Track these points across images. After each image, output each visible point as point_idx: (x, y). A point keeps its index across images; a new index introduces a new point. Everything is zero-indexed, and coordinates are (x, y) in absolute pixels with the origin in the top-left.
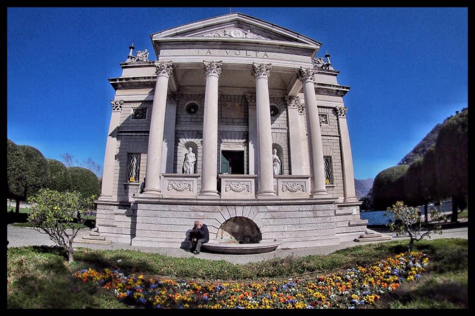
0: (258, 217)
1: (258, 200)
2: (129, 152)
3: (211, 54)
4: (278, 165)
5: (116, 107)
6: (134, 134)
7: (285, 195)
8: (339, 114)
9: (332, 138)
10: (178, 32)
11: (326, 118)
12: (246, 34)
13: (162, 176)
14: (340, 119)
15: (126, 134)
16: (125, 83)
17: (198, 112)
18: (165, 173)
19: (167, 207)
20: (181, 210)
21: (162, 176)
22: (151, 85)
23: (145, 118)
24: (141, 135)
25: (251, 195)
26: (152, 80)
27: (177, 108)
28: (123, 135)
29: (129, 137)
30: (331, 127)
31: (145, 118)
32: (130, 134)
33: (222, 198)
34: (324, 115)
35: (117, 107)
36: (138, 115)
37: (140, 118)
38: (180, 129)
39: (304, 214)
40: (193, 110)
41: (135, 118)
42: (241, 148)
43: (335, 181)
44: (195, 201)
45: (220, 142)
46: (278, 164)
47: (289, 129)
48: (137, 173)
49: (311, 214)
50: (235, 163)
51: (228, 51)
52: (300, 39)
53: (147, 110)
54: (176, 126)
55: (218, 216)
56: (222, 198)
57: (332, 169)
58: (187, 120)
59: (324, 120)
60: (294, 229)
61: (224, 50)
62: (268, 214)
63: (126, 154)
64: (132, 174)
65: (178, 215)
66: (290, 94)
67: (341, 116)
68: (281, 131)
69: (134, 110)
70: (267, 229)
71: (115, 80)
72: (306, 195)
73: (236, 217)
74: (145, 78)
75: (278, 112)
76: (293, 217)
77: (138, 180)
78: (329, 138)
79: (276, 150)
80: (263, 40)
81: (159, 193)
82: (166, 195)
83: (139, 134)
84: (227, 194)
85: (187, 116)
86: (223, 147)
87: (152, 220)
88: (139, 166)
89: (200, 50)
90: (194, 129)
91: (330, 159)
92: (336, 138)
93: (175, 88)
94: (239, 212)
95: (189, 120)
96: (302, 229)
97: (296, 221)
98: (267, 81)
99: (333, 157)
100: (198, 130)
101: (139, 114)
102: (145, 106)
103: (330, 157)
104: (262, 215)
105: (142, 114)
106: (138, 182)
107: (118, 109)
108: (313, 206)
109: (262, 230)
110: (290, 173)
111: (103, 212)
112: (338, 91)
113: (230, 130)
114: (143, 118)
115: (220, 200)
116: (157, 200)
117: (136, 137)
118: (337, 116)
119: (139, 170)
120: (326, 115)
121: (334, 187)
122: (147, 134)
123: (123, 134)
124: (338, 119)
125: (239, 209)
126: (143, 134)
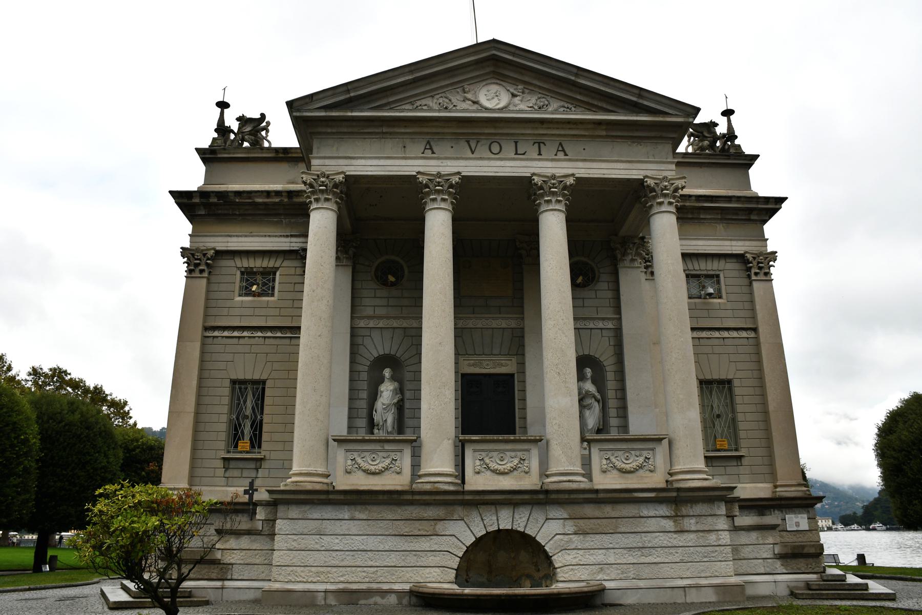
0: (548, 530)
2: (234, 377)
3: (433, 153)
4: (597, 407)
5: (197, 265)
6: (245, 334)
8: (753, 271)
9: (735, 334)
10: (352, 94)
11: (718, 282)
12: (514, 95)
13: (331, 442)
14: (755, 284)
15: (226, 334)
16: (215, 204)
18: (345, 434)
19: (345, 513)
21: (331, 442)
22: (291, 211)
23: (273, 295)
24: (265, 337)
25: (530, 482)
27: (353, 273)
28: (217, 337)
29: (235, 341)
31: (273, 295)
32: (236, 334)
33: (468, 487)
34: (711, 276)
35: (198, 265)
36: (254, 288)
37: (259, 295)
38: (362, 324)
39: (652, 524)
40: (392, 279)
41: (247, 295)
42: (507, 367)
43: (743, 443)
44: (409, 497)
46: (596, 404)
47: (620, 319)
48: (255, 430)
49: (669, 524)
50: (491, 407)
52: (646, 103)
53: (278, 274)
54: (352, 318)
58: (378, 302)
59: (711, 290)
60: (632, 560)
62: (570, 523)
63: (227, 383)
64: (243, 433)
66: (623, 232)
67: (761, 277)
69: (242, 273)
73: (499, 531)
74: (268, 193)
75: (593, 278)
77: (260, 447)
78: (725, 334)
79: (588, 372)
80: (555, 110)
81: (325, 480)
82: (343, 483)
83: (259, 334)
87: (311, 542)
88: (262, 413)
90: (395, 325)
91: (730, 389)
92: (744, 334)
93: (348, 224)
94: (505, 520)
95: (384, 302)
97: (633, 540)
98: (562, 217)
99: (736, 383)
100: (405, 325)
101: (258, 285)
102: (271, 265)
104: (554, 527)
105: (264, 284)
107: (202, 271)
109: (558, 560)
110: (625, 427)
112: (751, 211)
113: (480, 326)
114: (267, 295)
116: (323, 497)
117: (252, 341)
118: (749, 276)
119: (261, 421)
120: (718, 276)
121: (740, 458)
122: (279, 334)
123: (216, 333)
124: (751, 284)
126: (269, 334)
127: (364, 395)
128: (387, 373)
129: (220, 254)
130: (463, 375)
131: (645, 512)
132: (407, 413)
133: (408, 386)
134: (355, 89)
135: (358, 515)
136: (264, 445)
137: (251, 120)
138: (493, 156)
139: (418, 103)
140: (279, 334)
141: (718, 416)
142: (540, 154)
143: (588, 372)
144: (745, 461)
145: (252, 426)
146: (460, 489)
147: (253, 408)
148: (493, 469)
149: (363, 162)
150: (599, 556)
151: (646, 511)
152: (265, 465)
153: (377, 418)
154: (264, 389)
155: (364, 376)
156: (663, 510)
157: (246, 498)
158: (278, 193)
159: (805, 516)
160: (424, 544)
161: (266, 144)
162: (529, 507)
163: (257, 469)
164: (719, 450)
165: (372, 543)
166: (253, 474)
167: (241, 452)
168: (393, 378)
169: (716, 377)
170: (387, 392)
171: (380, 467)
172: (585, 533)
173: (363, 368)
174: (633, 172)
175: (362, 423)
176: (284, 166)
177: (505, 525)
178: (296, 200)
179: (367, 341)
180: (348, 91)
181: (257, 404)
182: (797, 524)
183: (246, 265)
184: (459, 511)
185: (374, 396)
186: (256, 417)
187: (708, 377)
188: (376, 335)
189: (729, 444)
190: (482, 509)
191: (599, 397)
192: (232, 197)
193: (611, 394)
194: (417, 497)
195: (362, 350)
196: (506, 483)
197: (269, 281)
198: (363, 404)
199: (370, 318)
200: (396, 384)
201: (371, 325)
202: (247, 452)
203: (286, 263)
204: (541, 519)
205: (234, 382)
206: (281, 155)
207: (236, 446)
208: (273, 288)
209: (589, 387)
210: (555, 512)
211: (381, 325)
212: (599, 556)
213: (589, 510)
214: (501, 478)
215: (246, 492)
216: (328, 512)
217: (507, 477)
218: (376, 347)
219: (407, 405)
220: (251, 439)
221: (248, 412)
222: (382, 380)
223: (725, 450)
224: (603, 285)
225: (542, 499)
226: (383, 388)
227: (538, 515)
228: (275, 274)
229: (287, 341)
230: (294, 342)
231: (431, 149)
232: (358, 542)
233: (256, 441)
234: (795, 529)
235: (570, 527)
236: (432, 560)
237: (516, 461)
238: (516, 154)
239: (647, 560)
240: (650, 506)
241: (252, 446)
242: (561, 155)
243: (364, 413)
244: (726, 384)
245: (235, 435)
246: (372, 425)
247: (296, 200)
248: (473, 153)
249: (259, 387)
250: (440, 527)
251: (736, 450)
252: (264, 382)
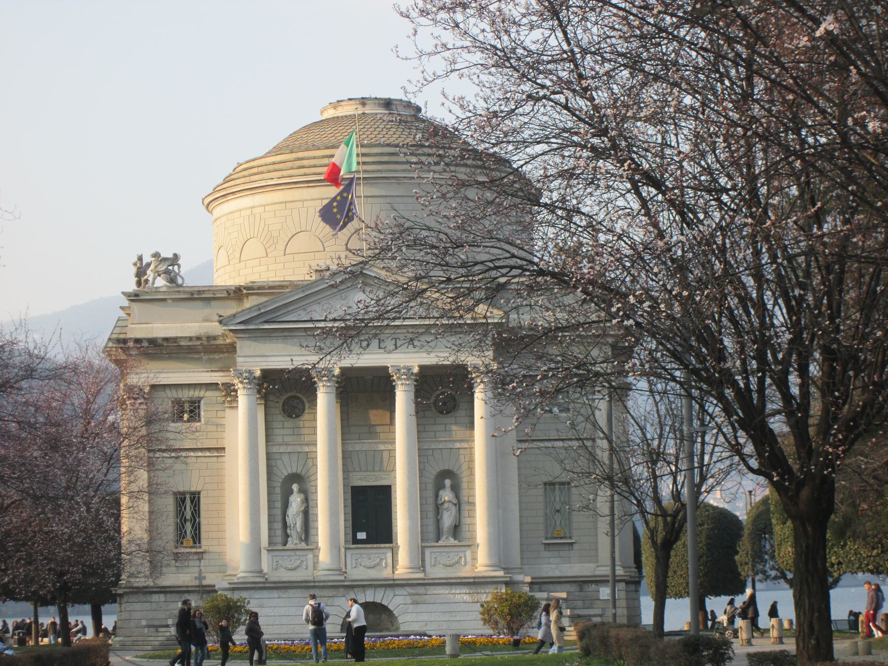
0: (395, 601)
1: (394, 580)
4: (454, 510)
10: (262, 311)
17: (306, 416)
19: (275, 594)
31: (200, 421)
37: (188, 421)
38: (274, 451)
44: (312, 584)
45: (346, 471)
53: (202, 402)
54: (267, 446)
62: (409, 597)
64: (186, 532)
69: (173, 402)
71: (125, 341)
74: (191, 339)
83: (192, 454)
85: (286, 424)
95: (290, 431)
104: (398, 600)
105: (191, 411)
106: (200, 547)
109: (401, 619)
111: (137, 606)
114: (195, 421)
119: (199, 523)
126: (200, 454)
127: (279, 505)
128: (295, 487)
129: (153, 387)
130: (352, 487)
132: (311, 517)
133: (311, 497)
134: (266, 307)
135: (282, 595)
136: (203, 542)
137: (165, 260)
139: (309, 309)
140: (208, 454)
141: (558, 511)
143: (448, 482)
144: (575, 547)
145: (192, 527)
147: (192, 513)
148: (368, 564)
149: (273, 359)
150: (425, 617)
152: (205, 556)
153: (289, 520)
154: (199, 498)
155: (278, 490)
156: (465, 590)
157: (197, 583)
158: (198, 338)
161: (180, 281)
162: (384, 589)
163: (200, 560)
164: (556, 538)
166: (197, 563)
167: (186, 547)
170: (296, 501)
171: (293, 566)
172: (417, 603)
173: (278, 485)
175: (278, 526)
176: (200, 303)
178: (212, 342)
179: (279, 462)
180: (260, 309)
181: (195, 510)
183: (175, 395)
184: (342, 590)
185: (286, 505)
186: (195, 520)
188: (285, 458)
190: (356, 590)
191: (455, 501)
192: (160, 341)
194: (317, 584)
195: (275, 470)
196: (373, 574)
197: (195, 408)
198: (278, 512)
199: (280, 445)
200: (302, 496)
201: (282, 451)
202: (191, 547)
203: (209, 394)
204: (391, 596)
205: (175, 494)
206: (196, 296)
207: (182, 543)
208: (199, 414)
209: (447, 495)
210: (398, 591)
211: (288, 450)
212: (425, 617)
213: (421, 590)
214: (369, 570)
215: (196, 578)
216: (265, 594)
217: (372, 570)
218: (286, 468)
219: (311, 512)
220: (193, 537)
221: (188, 515)
222: (292, 492)
223: (561, 538)
224: (461, 413)
225: (392, 585)
226: (292, 498)
227: (390, 593)
228: (199, 402)
229: (215, 459)
230: (220, 459)
233: (197, 538)
235: (409, 600)
237: (378, 560)
238: (380, 348)
239: (455, 619)
240: (457, 587)
241: (195, 543)
242: (411, 346)
243: (279, 518)
245: (180, 534)
246: (285, 525)
247: (212, 342)
249: (195, 498)
251: (571, 538)
252: (199, 493)
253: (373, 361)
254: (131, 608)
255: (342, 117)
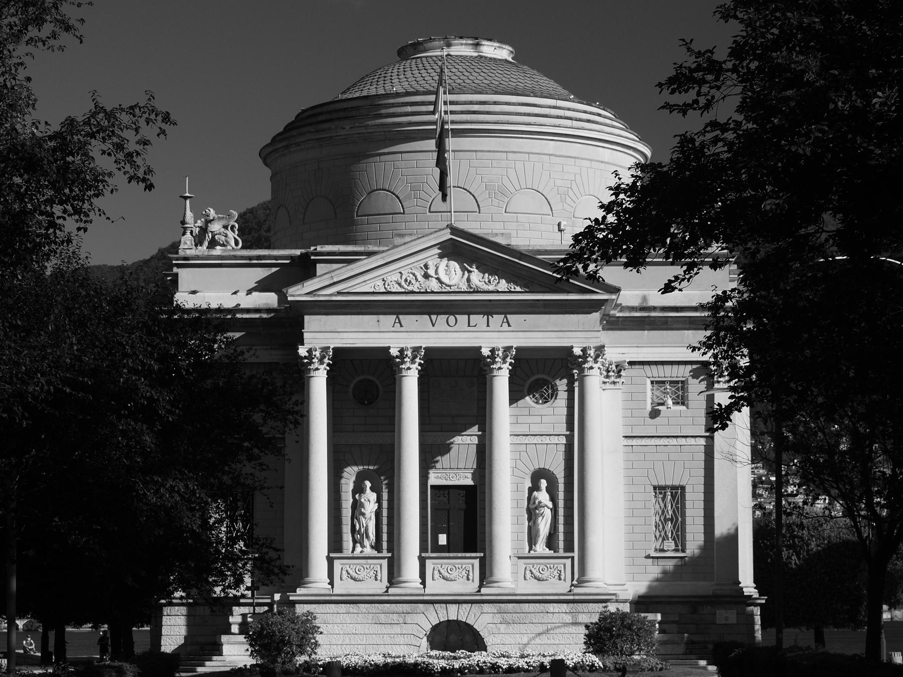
0: (481, 620)
7: (531, 588)
19: (343, 608)
20: (364, 610)
26: (265, 316)
30: (690, 413)
33: (428, 591)
39: (556, 619)
49: (568, 619)
51: (434, 317)
55: (420, 619)
56: (428, 591)
57: (683, 515)
61: (427, 317)
65: (360, 618)
68: (555, 440)
70: (495, 639)
72: (563, 587)
73: (448, 621)
76: (537, 621)
78: (682, 441)
84: (435, 587)
86: (434, 479)
89: (381, 317)
94: (453, 613)
96: (552, 642)
103: (683, 488)
104: (487, 618)
108: (571, 605)
115: (423, 595)
125: (453, 608)
131: (551, 610)
138: (450, 329)
142: (488, 326)
143: (544, 483)
146: (422, 592)
151: (551, 607)
159: (735, 611)
160: (397, 629)
165: (360, 629)
168: (372, 489)
169: (669, 483)
174: (565, 343)
177: (453, 617)
182: (727, 619)
187: (662, 483)
189: (676, 545)
190: (436, 606)
191: (550, 505)
193: (561, 504)
209: (543, 496)
210: (486, 607)
231: (400, 322)
232: (351, 628)
234: (724, 622)
236: (401, 639)
242: (505, 325)
244: (678, 493)
248: (433, 325)
250: (409, 619)
253: (463, 341)
254: (172, 623)
255: (491, 59)
